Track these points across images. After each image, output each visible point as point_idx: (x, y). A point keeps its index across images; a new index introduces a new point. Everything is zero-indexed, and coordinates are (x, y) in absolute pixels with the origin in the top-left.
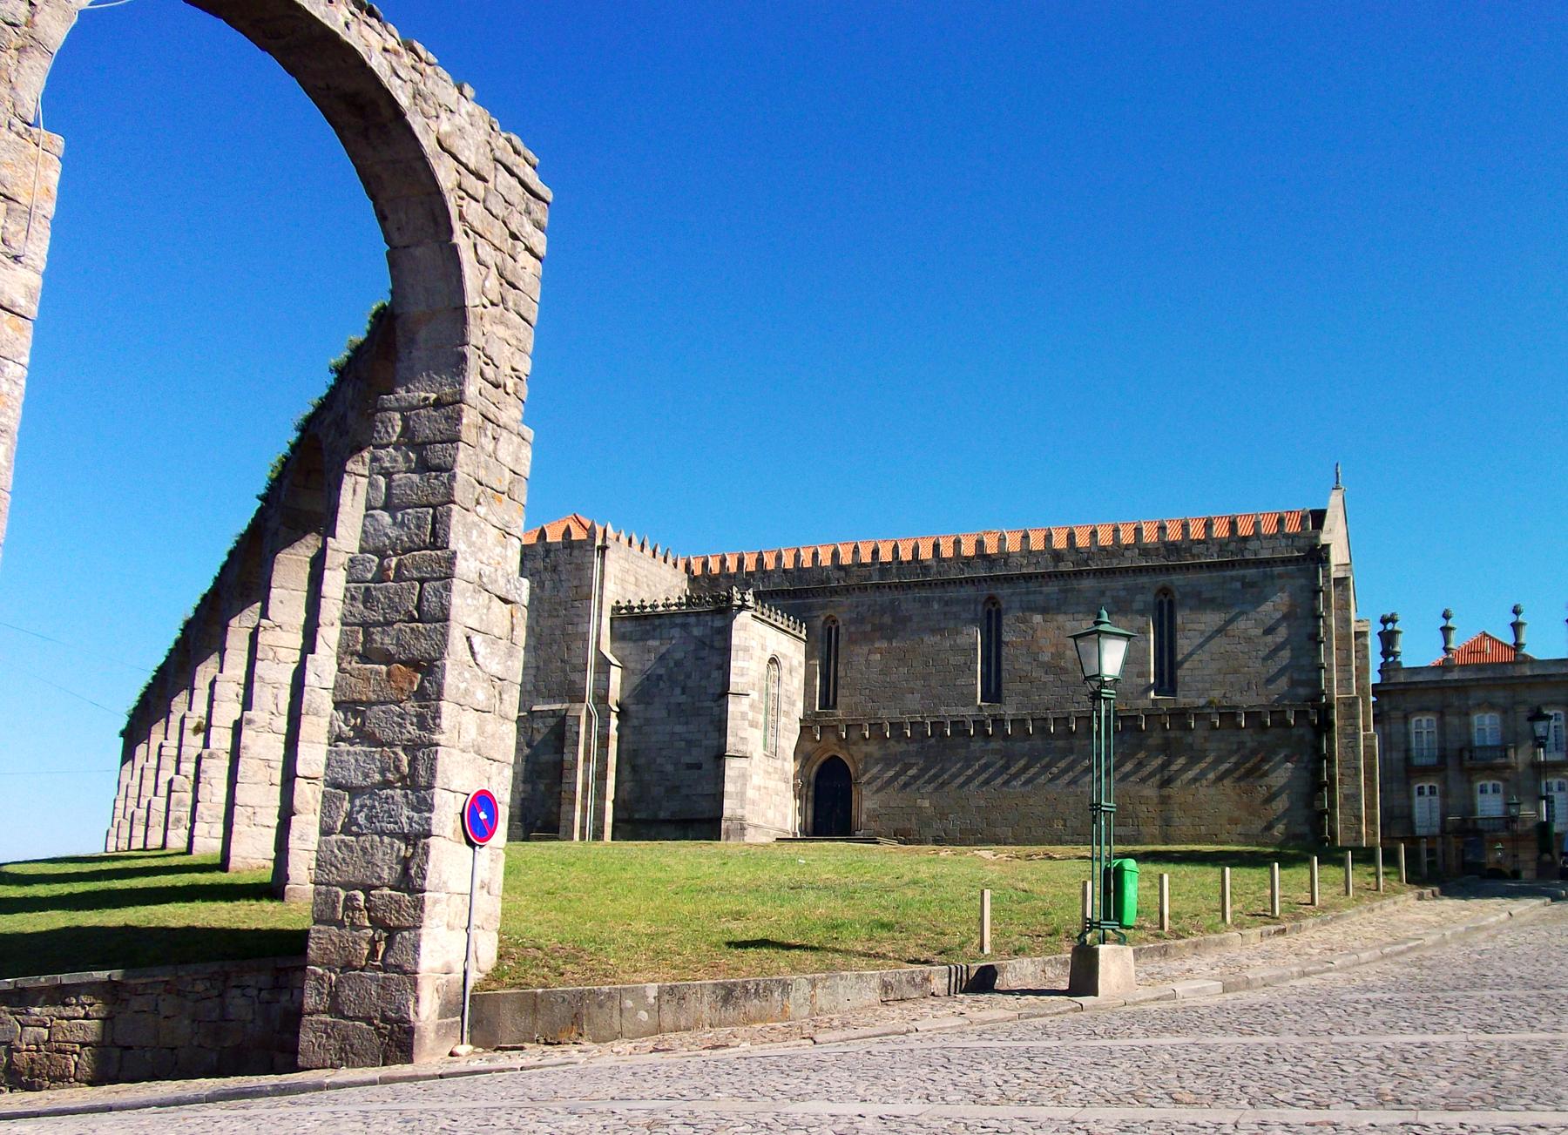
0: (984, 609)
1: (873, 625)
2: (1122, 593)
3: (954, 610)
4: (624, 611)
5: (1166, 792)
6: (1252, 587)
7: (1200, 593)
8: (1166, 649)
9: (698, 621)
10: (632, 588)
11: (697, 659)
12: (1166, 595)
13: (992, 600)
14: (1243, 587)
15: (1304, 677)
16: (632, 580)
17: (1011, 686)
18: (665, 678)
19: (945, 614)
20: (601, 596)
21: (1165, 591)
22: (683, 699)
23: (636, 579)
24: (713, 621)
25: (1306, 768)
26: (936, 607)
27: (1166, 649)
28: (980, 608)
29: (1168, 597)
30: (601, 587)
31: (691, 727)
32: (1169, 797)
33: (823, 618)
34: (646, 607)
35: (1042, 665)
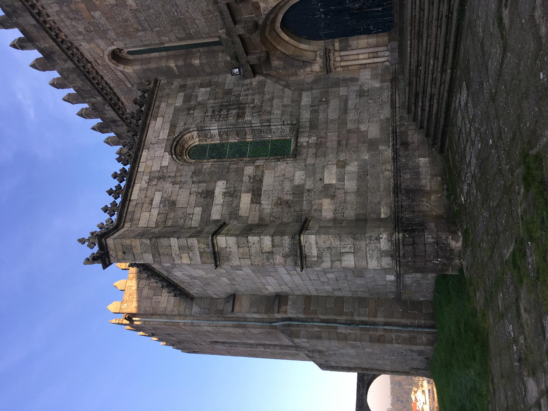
33: (121, 67)
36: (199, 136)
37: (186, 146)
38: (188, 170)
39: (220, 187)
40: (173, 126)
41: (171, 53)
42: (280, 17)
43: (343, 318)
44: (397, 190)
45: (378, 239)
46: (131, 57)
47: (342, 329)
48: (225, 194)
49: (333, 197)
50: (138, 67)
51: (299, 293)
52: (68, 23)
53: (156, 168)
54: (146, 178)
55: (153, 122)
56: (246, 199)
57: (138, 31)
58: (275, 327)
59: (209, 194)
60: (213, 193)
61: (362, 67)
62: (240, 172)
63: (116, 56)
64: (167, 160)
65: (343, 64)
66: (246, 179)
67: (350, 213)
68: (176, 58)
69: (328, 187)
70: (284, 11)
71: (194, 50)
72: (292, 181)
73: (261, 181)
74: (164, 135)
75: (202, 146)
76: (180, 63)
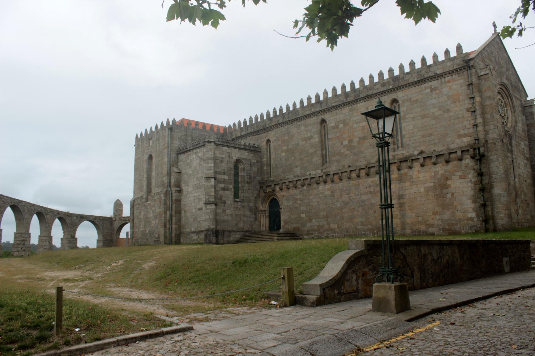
3: (309, 128)
5: (402, 201)
6: (435, 90)
7: (410, 99)
8: (399, 130)
9: (200, 150)
11: (200, 165)
12: (397, 103)
13: (323, 121)
14: (431, 91)
15: (466, 132)
18: (192, 174)
19: (306, 131)
24: (204, 150)
26: (303, 128)
27: (399, 130)
28: (319, 126)
29: (398, 104)
31: (200, 193)
32: (403, 203)
33: (265, 141)
35: (344, 146)
36: (242, 168)
37: (238, 164)
38: (232, 166)
39: (226, 177)
41: (269, 159)
43: (173, 213)
44: (224, 231)
45: (213, 225)
47: (168, 213)
48: (224, 179)
49: (223, 213)
50: (265, 147)
51: (183, 197)
53: (233, 154)
54: (229, 151)
55: (247, 152)
56: (222, 186)
57: (275, 153)
58: (168, 187)
59: (224, 174)
60: (225, 175)
62: (230, 183)
63: (268, 141)
64: (235, 158)
66: (228, 185)
67: (218, 218)
68: (267, 161)
69: (225, 211)
70: (277, 199)
71: (269, 168)
72: (227, 200)
73: (227, 190)
74: (243, 156)
75: (238, 169)
76: (265, 163)
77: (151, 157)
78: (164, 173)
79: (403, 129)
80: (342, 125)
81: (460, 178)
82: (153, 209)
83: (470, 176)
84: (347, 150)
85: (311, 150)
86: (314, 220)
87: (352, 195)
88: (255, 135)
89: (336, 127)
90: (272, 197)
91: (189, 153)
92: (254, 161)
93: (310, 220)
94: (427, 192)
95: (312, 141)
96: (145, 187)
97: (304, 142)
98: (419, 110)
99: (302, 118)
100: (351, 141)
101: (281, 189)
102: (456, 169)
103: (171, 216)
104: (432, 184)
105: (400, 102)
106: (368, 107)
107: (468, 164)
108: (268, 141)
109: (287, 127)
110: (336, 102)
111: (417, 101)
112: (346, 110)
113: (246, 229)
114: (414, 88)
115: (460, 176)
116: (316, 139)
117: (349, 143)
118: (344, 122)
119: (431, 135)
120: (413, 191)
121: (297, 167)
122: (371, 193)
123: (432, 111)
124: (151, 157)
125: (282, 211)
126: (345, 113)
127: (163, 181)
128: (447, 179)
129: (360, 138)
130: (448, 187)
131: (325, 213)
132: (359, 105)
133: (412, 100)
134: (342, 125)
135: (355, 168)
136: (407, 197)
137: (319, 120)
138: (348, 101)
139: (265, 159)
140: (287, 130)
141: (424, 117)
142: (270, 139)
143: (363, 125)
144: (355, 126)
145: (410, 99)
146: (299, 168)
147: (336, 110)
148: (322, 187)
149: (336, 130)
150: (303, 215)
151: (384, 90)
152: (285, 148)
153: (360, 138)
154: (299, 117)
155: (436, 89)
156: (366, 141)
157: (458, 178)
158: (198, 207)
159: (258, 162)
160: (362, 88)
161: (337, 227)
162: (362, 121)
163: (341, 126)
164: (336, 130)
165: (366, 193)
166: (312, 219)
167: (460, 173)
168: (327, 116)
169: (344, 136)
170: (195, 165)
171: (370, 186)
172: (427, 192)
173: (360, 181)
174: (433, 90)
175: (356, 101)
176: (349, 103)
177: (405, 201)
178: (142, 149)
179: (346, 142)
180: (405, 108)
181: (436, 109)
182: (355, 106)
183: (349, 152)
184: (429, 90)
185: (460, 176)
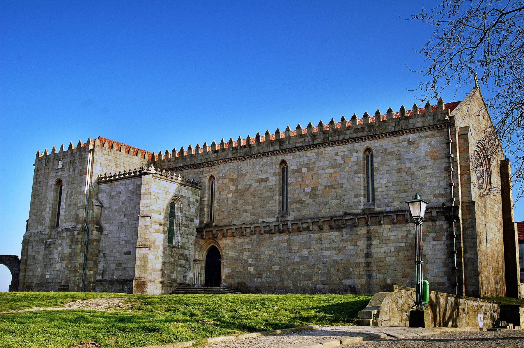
0: (280, 167)
1: (229, 179)
2: (347, 153)
4: (103, 179)
5: (369, 260)
6: (413, 144)
7: (386, 150)
8: (370, 181)
10: (114, 168)
12: (370, 152)
13: (283, 162)
14: (408, 144)
16: (114, 164)
17: (292, 206)
20: (92, 173)
21: (368, 150)
22: (125, 220)
23: (116, 164)
25: (444, 243)
27: (370, 181)
28: (278, 167)
29: (371, 153)
30: (92, 169)
33: (208, 177)
34: (111, 177)
35: (307, 194)
37: (175, 201)
40: (184, 197)
42: (217, 246)
46: (211, 182)
52: (227, 168)
55: (185, 188)
61: (194, 274)
65: (196, 267)
70: (219, 249)
76: (206, 203)
77: (59, 182)
78: (79, 205)
79: (375, 182)
80: (306, 169)
81: (434, 240)
82: (60, 248)
83: (444, 238)
84: (310, 198)
85: (266, 194)
86: (264, 276)
87: (312, 250)
88: (194, 168)
89: (299, 171)
90: (212, 245)
91: (116, 183)
92: (192, 200)
93: (260, 276)
94: (398, 252)
95: (268, 183)
96: (47, 220)
97: (258, 184)
98: (394, 163)
99: (257, 156)
100: (314, 189)
101: (225, 236)
102: (430, 230)
103: (86, 259)
104: (404, 244)
105: (374, 152)
106: (337, 153)
107: (442, 225)
108: (212, 177)
109: (237, 163)
110: (300, 142)
111: (392, 153)
112: (311, 154)
113: (178, 281)
114: (390, 139)
115: (433, 237)
116: (274, 181)
117: (312, 191)
118: (308, 166)
119: (406, 191)
120: (382, 250)
121: (246, 211)
122: (334, 249)
123: (408, 165)
124: (59, 182)
125: (224, 262)
126: (309, 157)
127: (77, 215)
128: (419, 240)
129: (325, 186)
130: (420, 248)
131: (278, 268)
132: (327, 149)
133: (388, 151)
134: (306, 169)
135: (318, 220)
136: (375, 256)
137: (279, 162)
138: (315, 143)
139: (206, 199)
140: (238, 167)
141: (399, 171)
142: (214, 175)
143: (330, 172)
144: (320, 172)
145: (386, 150)
146: (249, 214)
147: (300, 151)
148: (275, 238)
149: (298, 174)
150: (252, 269)
151: (357, 136)
152: (233, 188)
153: (325, 186)
154: (254, 153)
155: (414, 142)
156: (333, 190)
157: (431, 239)
158: (126, 250)
159: (197, 201)
160: (331, 131)
161: (292, 285)
162: (329, 168)
163: (304, 170)
164: (298, 174)
165: (329, 249)
166: (262, 275)
167: (434, 235)
168: (288, 158)
169: (307, 182)
170: (124, 199)
171: (334, 241)
172: (398, 252)
173: (324, 235)
174: (410, 143)
175: (323, 144)
176: (316, 145)
177: (373, 260)
178: (47, 171)
179: (308, 190)
180: (379, 159)
181: (412, 165)
182: (322, 149)
183: (312, 200)
184: (406, 143)
185: (433, 237)
